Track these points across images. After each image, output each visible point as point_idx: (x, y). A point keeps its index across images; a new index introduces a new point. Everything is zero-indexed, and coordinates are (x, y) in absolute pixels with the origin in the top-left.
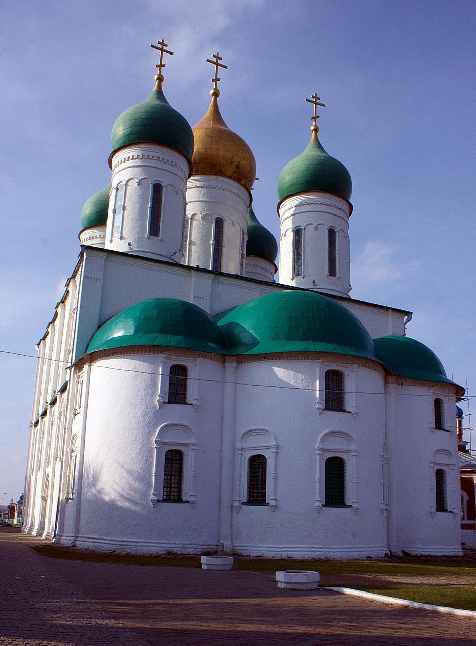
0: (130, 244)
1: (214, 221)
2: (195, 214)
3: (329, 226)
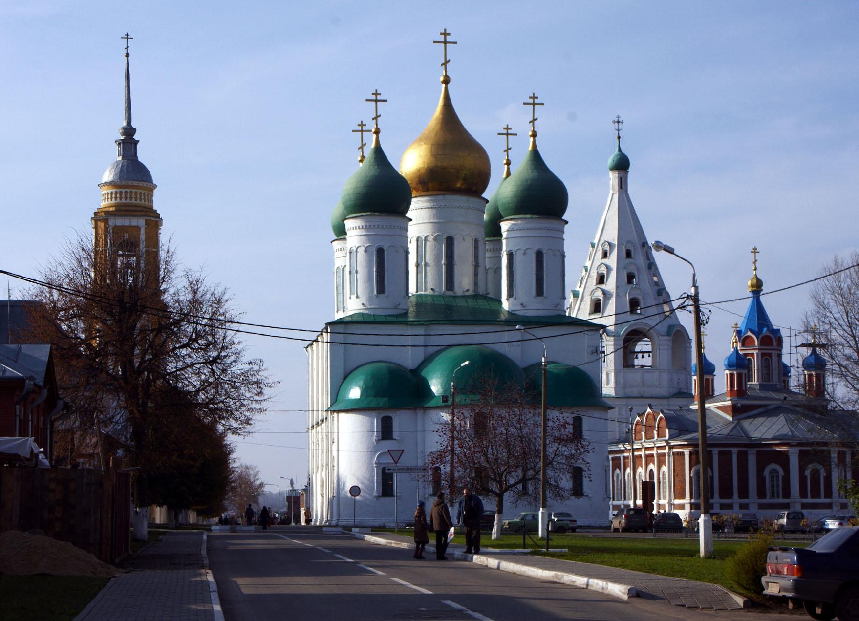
0: (363, 304)
1: (444, 241)
2: (427, 236)
3: (536, 248)
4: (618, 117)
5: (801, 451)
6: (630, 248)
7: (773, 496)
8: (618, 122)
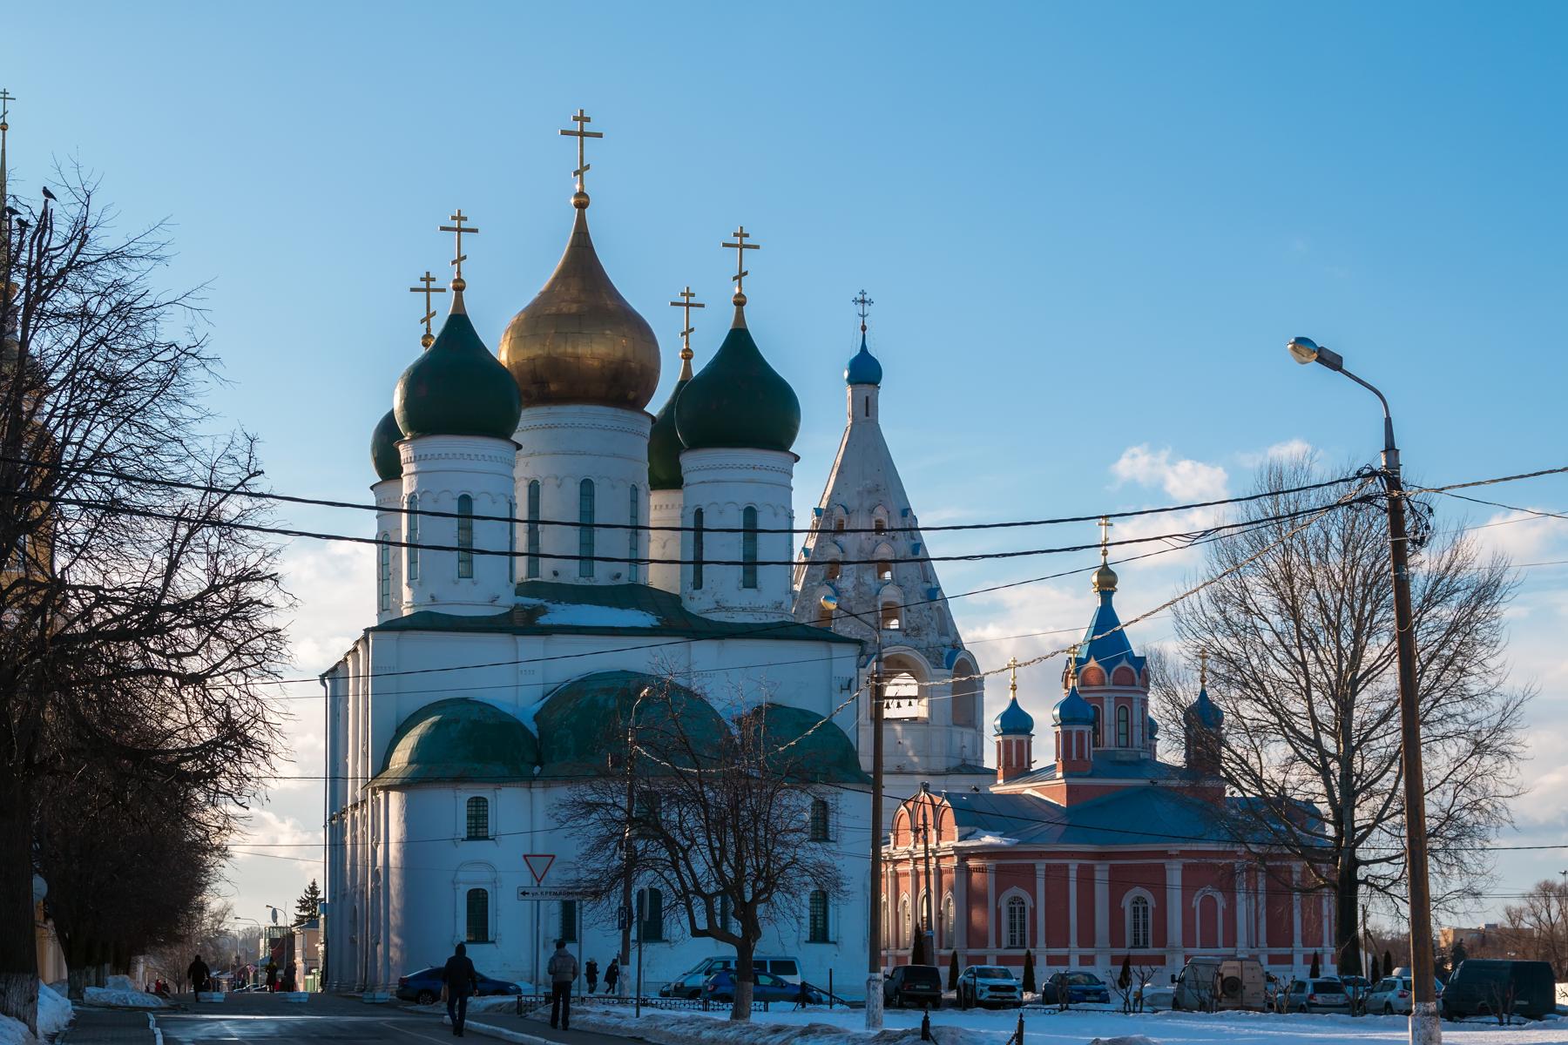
4: (863, 293)
6: (883, 518)
7: (1136, 944)
8: (863, 301)
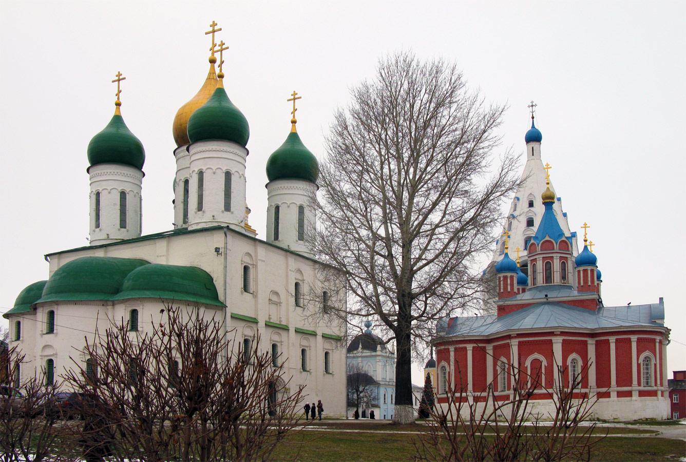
4: (532, 102)
5: (564, 340)
